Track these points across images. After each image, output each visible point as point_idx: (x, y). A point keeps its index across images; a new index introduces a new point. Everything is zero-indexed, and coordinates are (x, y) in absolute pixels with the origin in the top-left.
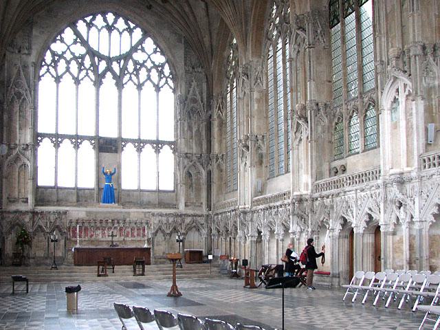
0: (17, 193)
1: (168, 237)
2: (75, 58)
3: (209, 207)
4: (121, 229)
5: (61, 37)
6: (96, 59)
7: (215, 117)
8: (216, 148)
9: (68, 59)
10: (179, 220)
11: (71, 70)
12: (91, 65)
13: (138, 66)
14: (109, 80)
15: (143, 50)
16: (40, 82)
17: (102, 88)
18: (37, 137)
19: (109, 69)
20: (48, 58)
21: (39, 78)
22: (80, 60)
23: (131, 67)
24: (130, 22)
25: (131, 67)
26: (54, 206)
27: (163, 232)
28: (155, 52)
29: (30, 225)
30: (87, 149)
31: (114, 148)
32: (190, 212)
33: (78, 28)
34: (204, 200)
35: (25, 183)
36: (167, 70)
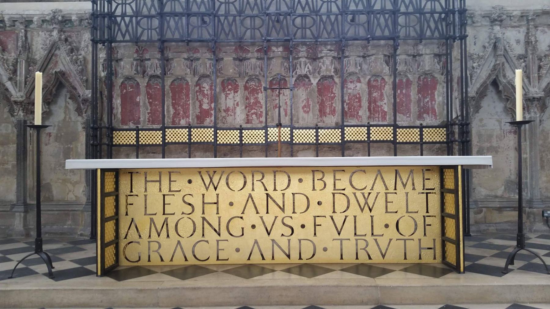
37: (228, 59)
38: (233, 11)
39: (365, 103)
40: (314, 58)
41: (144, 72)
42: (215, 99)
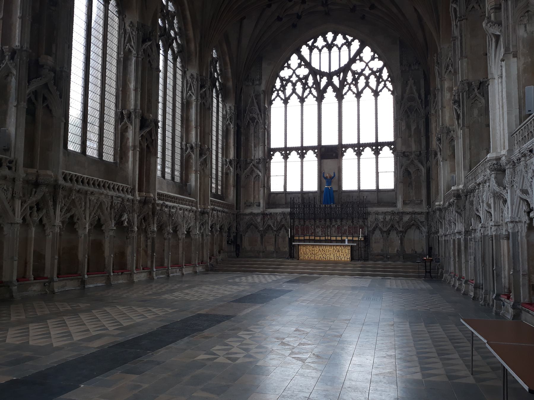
0: (252, 199)
1: (385, 235)
2: (300, 80)
4: (338, 228)
5: (288, 64)
6: (318, 77)
9: (294, 81)
11: (297, 91)
12: (314, 83)
13: (357, 76)
14: (330, 94)
15: (361, 60)
16: (272, 106)
18: (269, 153)
19: (330, 83)
20: (278, 84)
21: (271, 103)
22: (304, 81)
24: (347, 36)
26: (283, 208)
27: (381, 230)
28: (373, 58)
29: (261, 224)
30: (311, 157)
32: (409, 209)
33: (302, 53)
34: (424, 198)
35: (259, 191)
36: (385, 74)
37: (317, 222)
38: (319, 212)
39: (348, 231)
41: (300, 224)
42: (315, 230)
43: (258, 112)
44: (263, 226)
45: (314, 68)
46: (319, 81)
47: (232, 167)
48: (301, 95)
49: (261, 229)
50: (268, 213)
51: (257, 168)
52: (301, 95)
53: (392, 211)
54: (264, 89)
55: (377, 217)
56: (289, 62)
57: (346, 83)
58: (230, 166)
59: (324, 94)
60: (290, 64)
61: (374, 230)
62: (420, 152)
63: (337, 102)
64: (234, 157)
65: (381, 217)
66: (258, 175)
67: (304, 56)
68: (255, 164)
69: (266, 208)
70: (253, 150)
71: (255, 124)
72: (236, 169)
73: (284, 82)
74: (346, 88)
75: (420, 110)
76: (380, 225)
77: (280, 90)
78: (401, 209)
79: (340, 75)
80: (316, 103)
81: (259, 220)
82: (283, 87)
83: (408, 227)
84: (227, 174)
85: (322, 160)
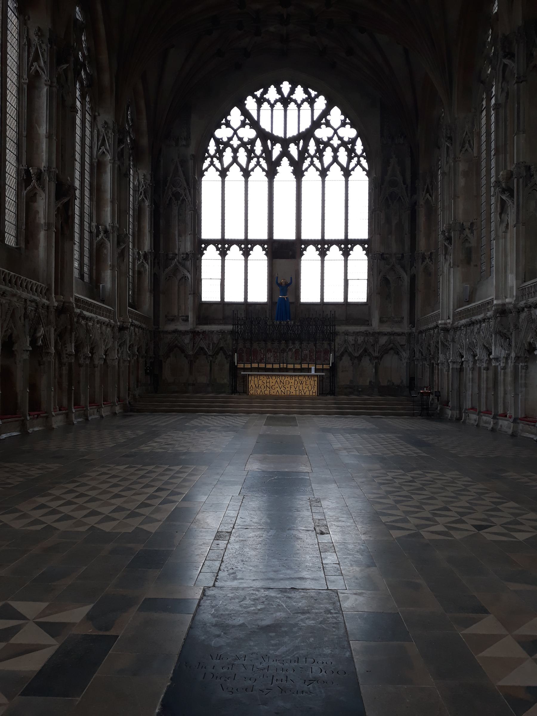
3: (412, 322)
5: (226, 120)
6: (269, 142)
7: (422, 202)
8: (422, 244)
9: (235, 146)
10: (371, 339)
11: (239, 160)
12: (263, 151)
15: (328, 124)
16: (204, 179)
17: (277, 178)
19: (285, 153)
20: (212, 148)
22: (249, 147)
23: (312, 147)
24: (310, 90)
25: (312, 147)
26: (221, 324)
27: (350, 354)
28: (343, 124)
31: (291, 253)
32: (386, 329)
33: (247, 107)
36: (359, 147)
39: (308, 357)
40: (294, 344)
43: (186, 186)
44: (193, 348)
45: (264, 130)
46: (270, 149)
47: (148, 263)
48: (244, 166)
49: (191, 353)
50: (200, 331)
51: (184, 266)
52: (244, 166)
53: (366, 331)
54: (193, 153)
55: (347, 338)
56: (229, 118)
57: (306, 155)
58: (144, 262)
59: (278, 168)
60: (229, 121)
61: (342, 355)
62: (403, 254)
63: (295, 180)
64: (151, 248)
65: (351, 339)
66: (185, 278)
67: (250, 111)
68: (180, 261)
69: (197, 325)
70: (177, 240)
71: (179, 202)
72: (154, 267)
73: (221, 146)
74: (307, 162)
75: (404, 199)
76: (350, 349)
77: (214, 156)
78: (378, 328)
79: (299, 143)
80: (266, 179)
81: (187, 341)
82: (220, 153)
83: (385, 351)
84: (140, 273)
85: (274, 260)
